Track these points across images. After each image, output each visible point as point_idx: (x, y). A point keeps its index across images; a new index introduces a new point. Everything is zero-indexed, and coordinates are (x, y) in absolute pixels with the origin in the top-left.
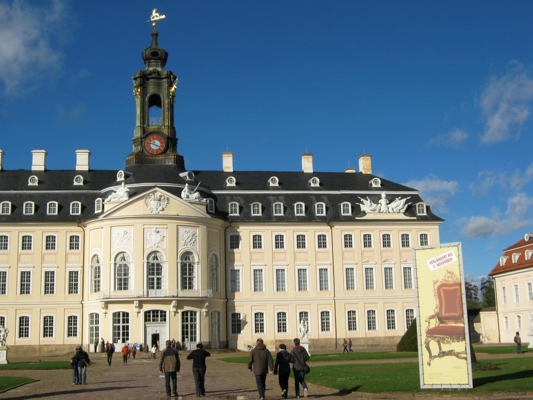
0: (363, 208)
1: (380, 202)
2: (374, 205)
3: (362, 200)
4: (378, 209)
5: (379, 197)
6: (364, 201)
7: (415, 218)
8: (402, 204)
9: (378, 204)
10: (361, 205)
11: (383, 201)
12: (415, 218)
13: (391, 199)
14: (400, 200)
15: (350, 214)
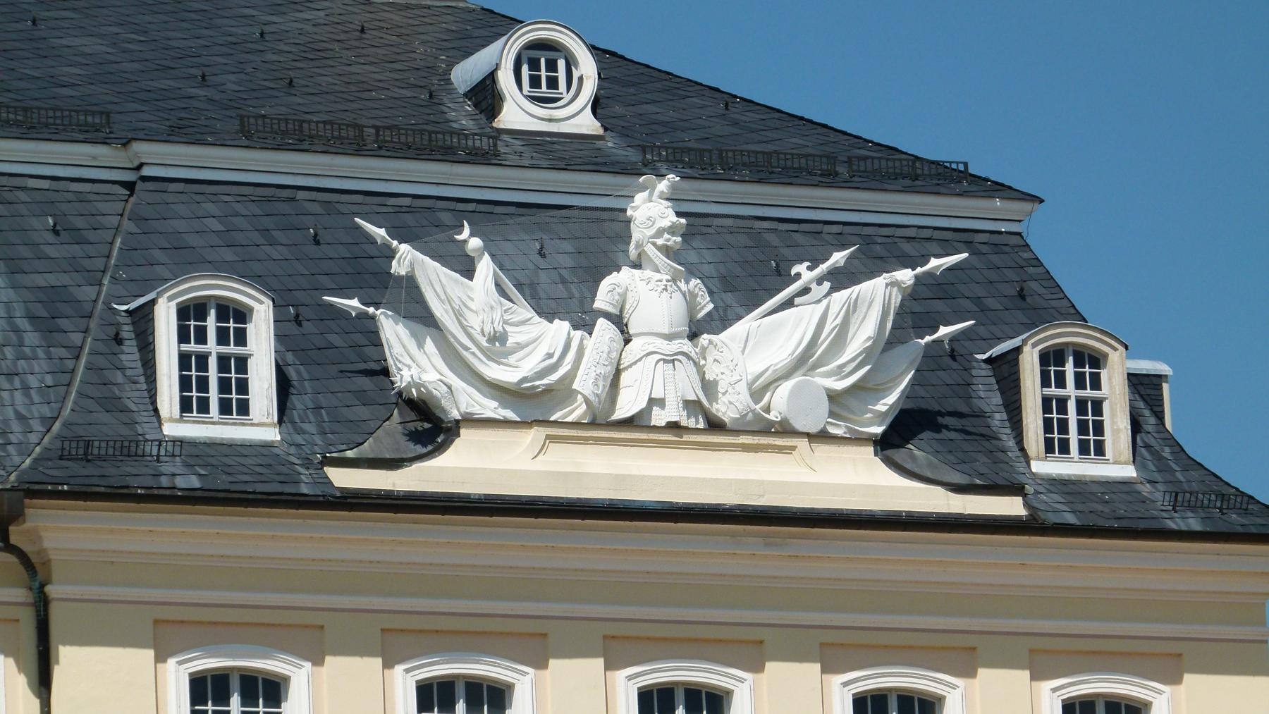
0: (414, 363)
1: (604, 298)
2: (539, 342)
3: (406, 259)
4: (587, 383)
5: (606, 243)
6: (434, 279)
7: (1011, 506)
8: (864, 333)
9: (584, 321)
10: (394, 333)
11: (649, 293)
12: (1011, 506)
13: (739, 272)
14: (840, 279)
15: (260, 425)
